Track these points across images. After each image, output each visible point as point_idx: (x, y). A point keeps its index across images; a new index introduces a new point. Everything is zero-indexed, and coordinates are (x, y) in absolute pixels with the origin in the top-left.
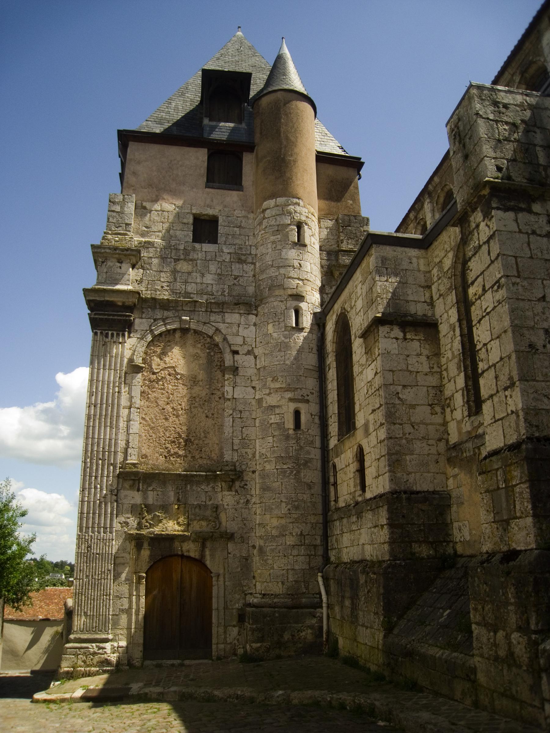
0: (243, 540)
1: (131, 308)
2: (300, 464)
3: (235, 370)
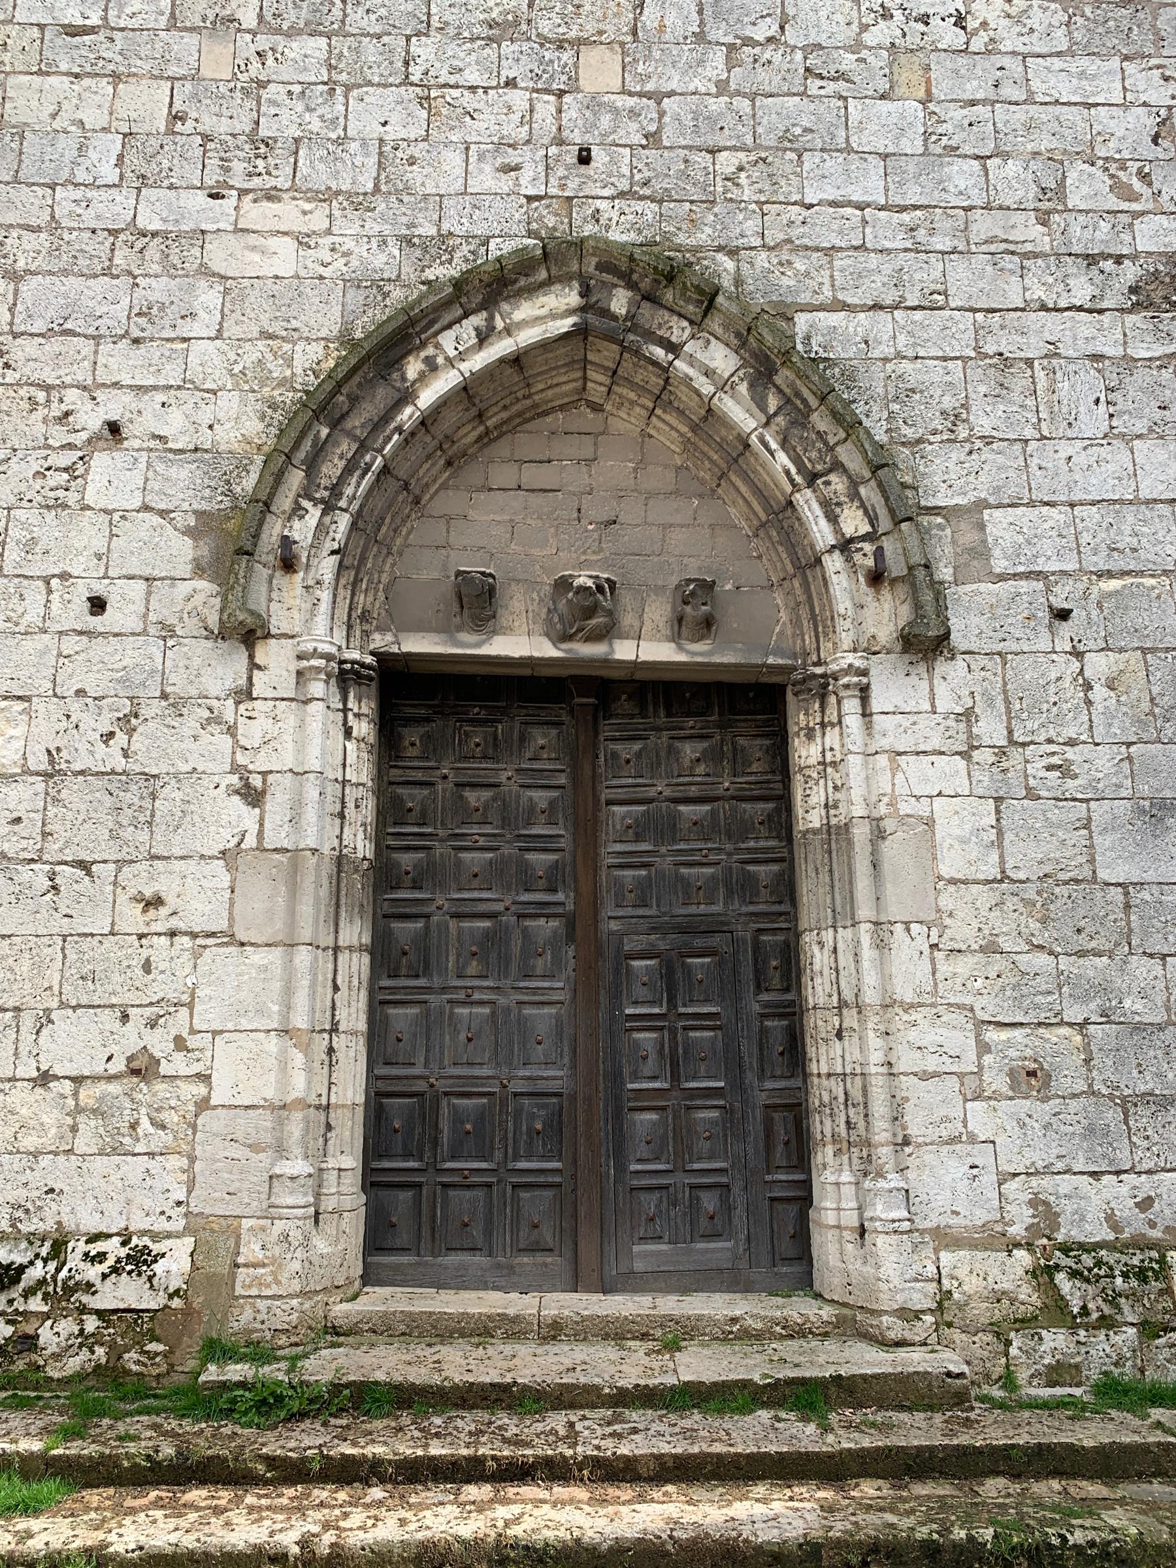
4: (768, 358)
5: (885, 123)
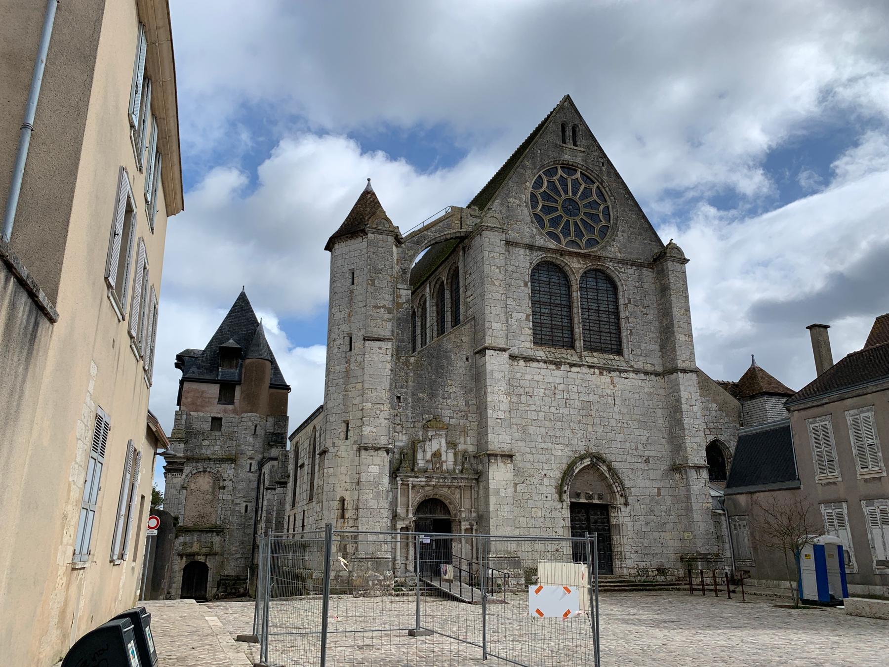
0: (222, 555)
1: (183, 464)
2: (245, 525)
3: (224, 488)
4: (610, 469)
5: (620, 437)
